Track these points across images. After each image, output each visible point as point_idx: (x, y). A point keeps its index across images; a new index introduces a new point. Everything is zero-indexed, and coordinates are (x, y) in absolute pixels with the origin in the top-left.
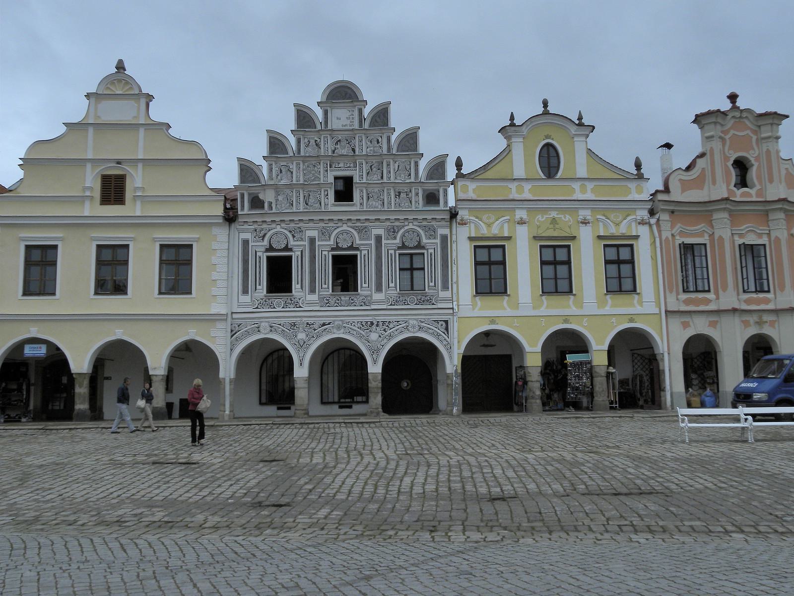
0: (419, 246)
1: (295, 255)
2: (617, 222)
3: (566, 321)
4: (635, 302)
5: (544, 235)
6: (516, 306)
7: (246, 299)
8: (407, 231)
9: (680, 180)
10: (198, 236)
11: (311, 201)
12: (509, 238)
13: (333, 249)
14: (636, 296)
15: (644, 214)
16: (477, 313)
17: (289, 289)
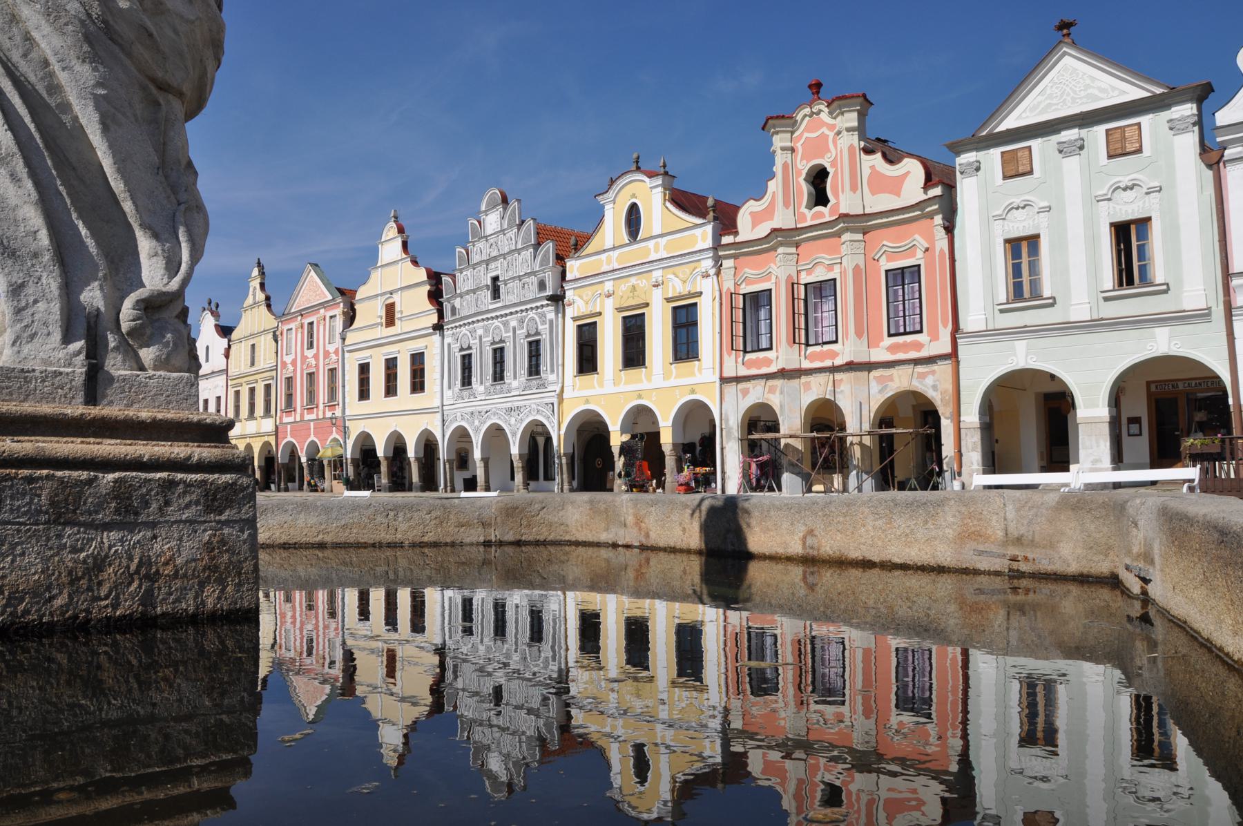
0: (537, 333)
1: (473, 351)
2: (684, 279)
3: (640, 396)
4: (696, 369)
5: (625, 305)
6: (601, 385)
7: (448, 393)
8: (530, 320)
9: (751, 213)
10: (424, 345)
11: (479, 302)
12: (600, 314)
13: (492, 344)
14: (697, 363)
15: (707, 264)
16: (577, 394)
17: (470, 383)
